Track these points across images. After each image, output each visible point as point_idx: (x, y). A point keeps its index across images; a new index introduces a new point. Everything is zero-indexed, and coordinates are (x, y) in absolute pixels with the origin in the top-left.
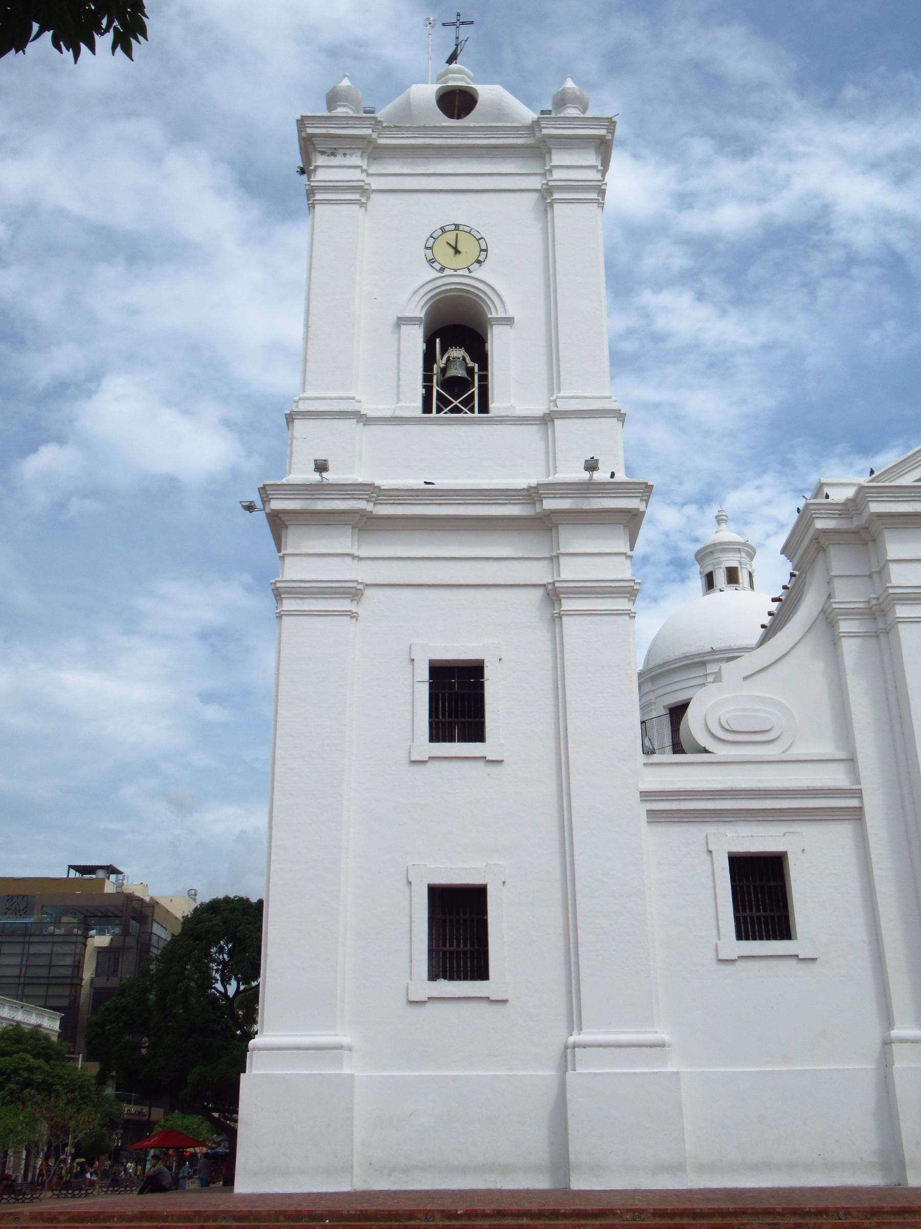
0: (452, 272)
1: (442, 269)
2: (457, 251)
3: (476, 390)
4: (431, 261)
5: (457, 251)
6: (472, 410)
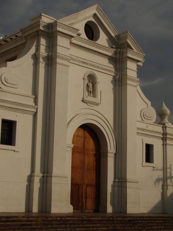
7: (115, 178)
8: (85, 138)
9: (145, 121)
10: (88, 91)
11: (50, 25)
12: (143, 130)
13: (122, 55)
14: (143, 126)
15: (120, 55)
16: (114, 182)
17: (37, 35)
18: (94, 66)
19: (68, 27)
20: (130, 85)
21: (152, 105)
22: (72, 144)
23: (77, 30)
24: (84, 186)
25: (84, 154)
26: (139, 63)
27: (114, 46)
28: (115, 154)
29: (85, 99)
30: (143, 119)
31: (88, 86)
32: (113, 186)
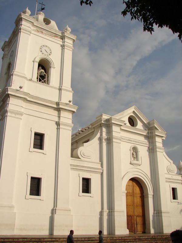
3: (46, 79)
7: (154, 211)
8: (133, 186)
11: (108, 120)
12: (169, 179)
13: (152, 134)
14: (169, 176)
15: (151, 134)
16: (154, 213)
17: (101, 126)
18: (136, 142)
21: (174, 163)
24: (135, 217)
25: (134, 196)
26: (163, 138)
27: (147, 129)
28: (153, 196)
29: (132, 162)
30: (169, 172)
31: (133, 154)
32: (153, 216)
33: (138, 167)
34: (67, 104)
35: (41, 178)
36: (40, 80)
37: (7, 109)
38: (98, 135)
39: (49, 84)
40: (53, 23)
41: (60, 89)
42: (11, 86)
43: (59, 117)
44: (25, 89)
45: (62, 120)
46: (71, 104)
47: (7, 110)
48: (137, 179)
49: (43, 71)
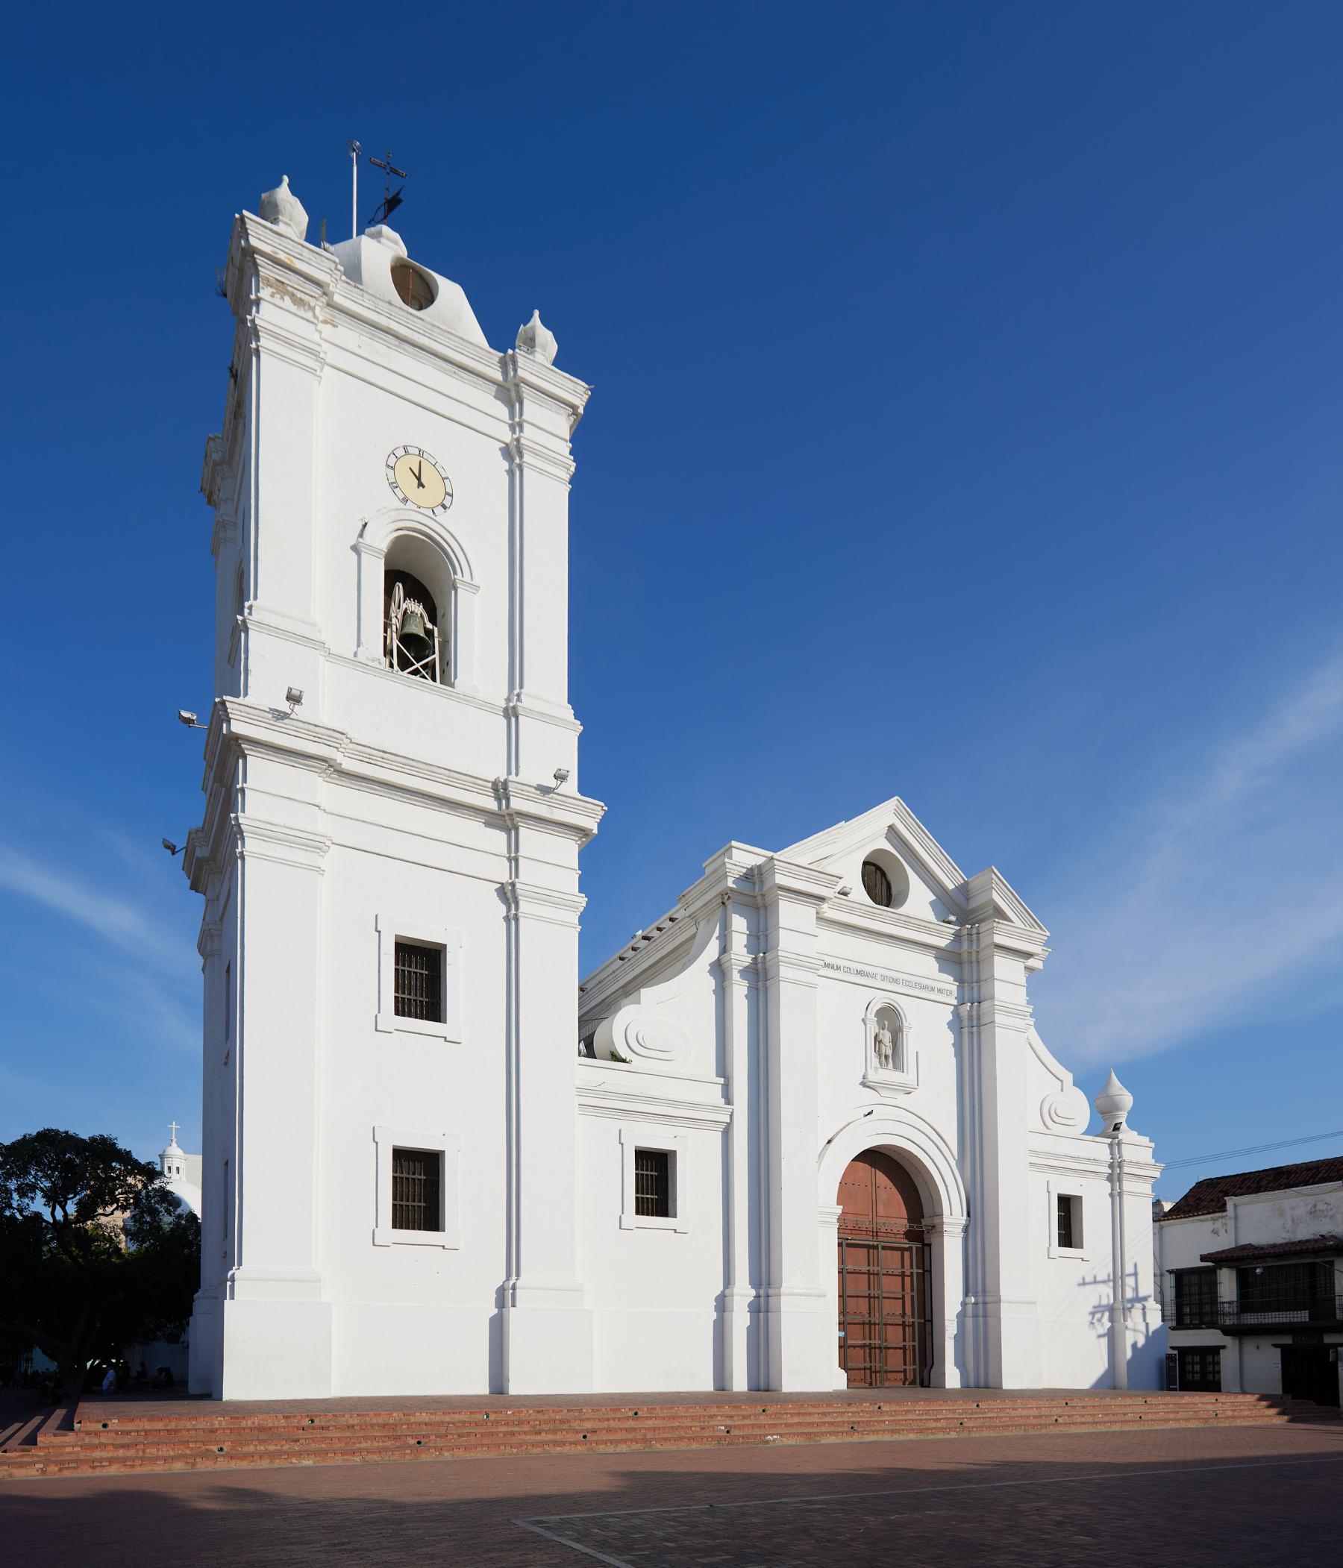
0: (415, 507)
1: (405, 500)
2: (421, 485)
3: (436, 656)
4: (394, 486)
5: (421, 485)
6: (434, 679)
9: (1056, 1129)
10: (880, 1055)
11: (756, 872)
12: (1048, 1155)
14: (1047, 1144)
18: (895, 981)
19: (811, 871)
20: (1007, 1027)
22: (838, 1204)
23: (837, 877)
27: (952, 918)
29: (872, 1077)
33: (901, 1100)
34: (545, 790)
35: (443, 1152)
36: (404, 664)
37: (237, 818)
38: (711, 951)
39: (452, 685)
40: (450, 294)
41: (511, 713)
42: (246, 694)
43: (514, 860)
44: (316, 710)
45: (529, 876)
46: (571, 786)
47: (239, 825)
48: (895, 1157)
49: (417, 608)
